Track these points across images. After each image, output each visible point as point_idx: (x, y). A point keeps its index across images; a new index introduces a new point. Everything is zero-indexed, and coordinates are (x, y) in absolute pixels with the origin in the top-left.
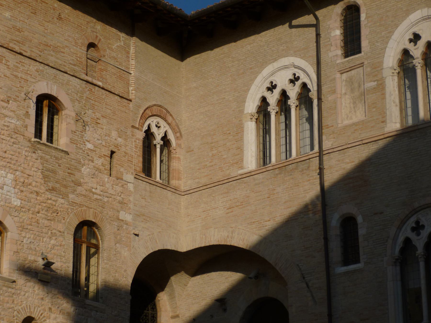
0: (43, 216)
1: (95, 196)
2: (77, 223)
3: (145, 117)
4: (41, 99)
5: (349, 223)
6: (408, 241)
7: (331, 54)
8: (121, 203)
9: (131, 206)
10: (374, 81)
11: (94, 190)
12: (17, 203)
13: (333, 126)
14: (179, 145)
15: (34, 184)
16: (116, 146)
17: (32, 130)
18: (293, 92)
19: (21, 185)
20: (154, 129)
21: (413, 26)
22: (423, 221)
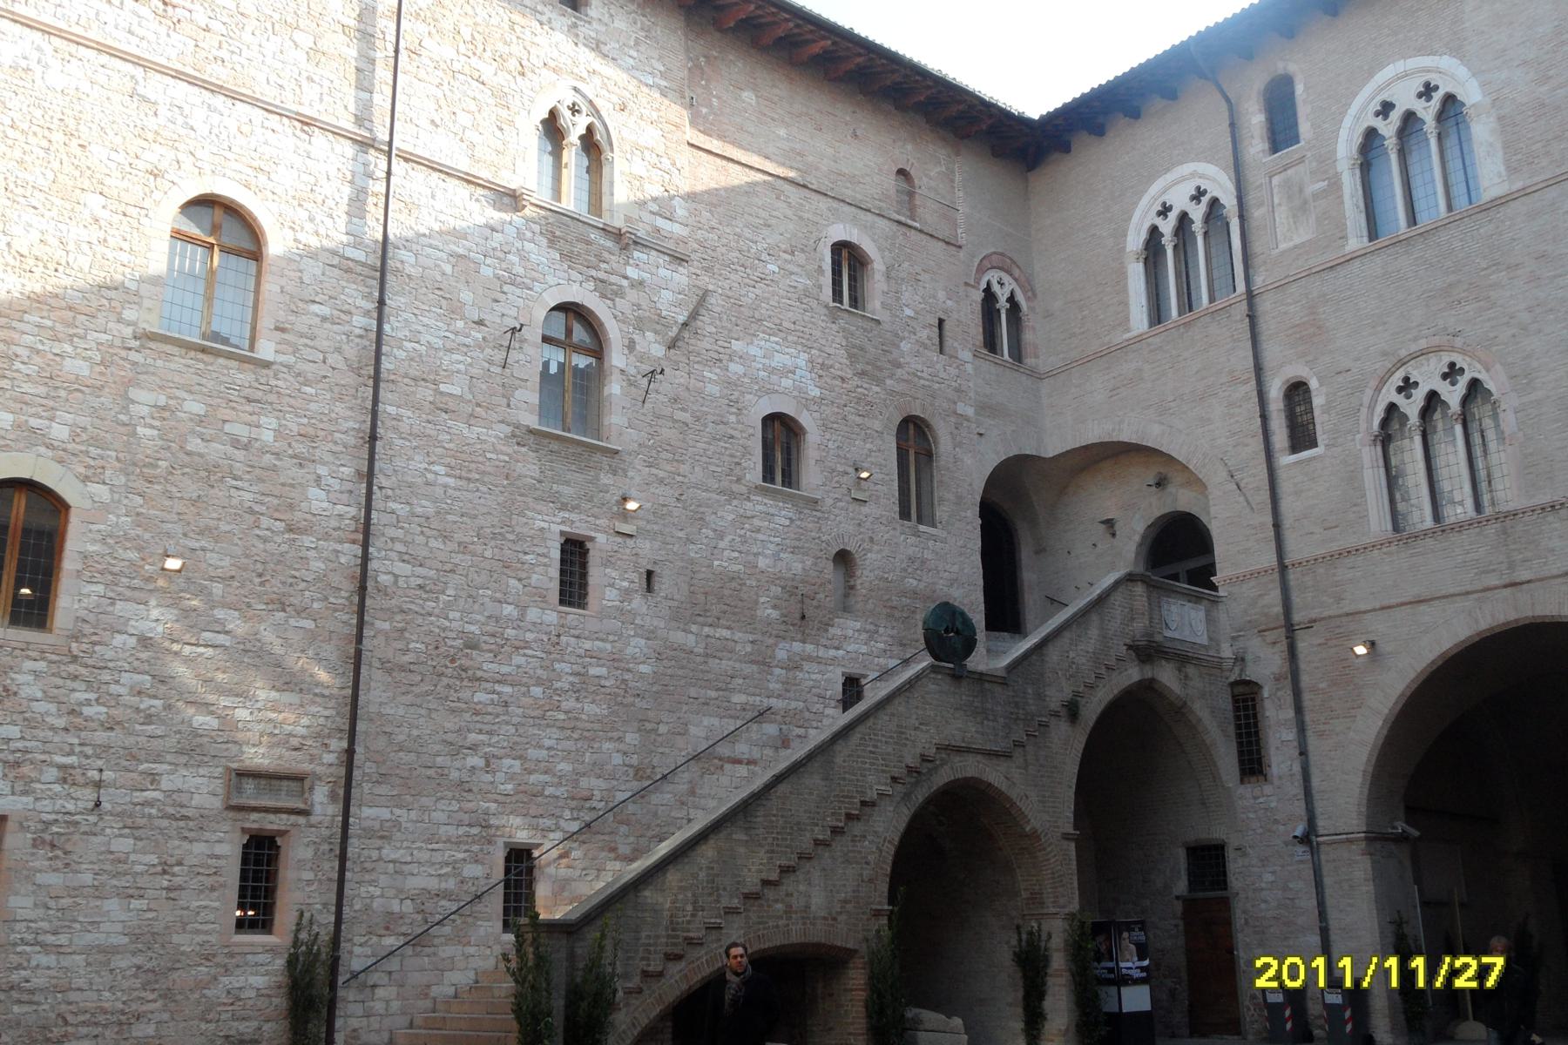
3: (981, 270)
4: (840, 248)
5: (1297, 391)
6: (1392, 408)
8: (958, 390)
9: (972, 394)
12: (816, 392)
14: (1031, 309)
16: (945, 311)
17: (828, 291)
18: (1197, 213)
19: (821, 368)
20: (996, 288)
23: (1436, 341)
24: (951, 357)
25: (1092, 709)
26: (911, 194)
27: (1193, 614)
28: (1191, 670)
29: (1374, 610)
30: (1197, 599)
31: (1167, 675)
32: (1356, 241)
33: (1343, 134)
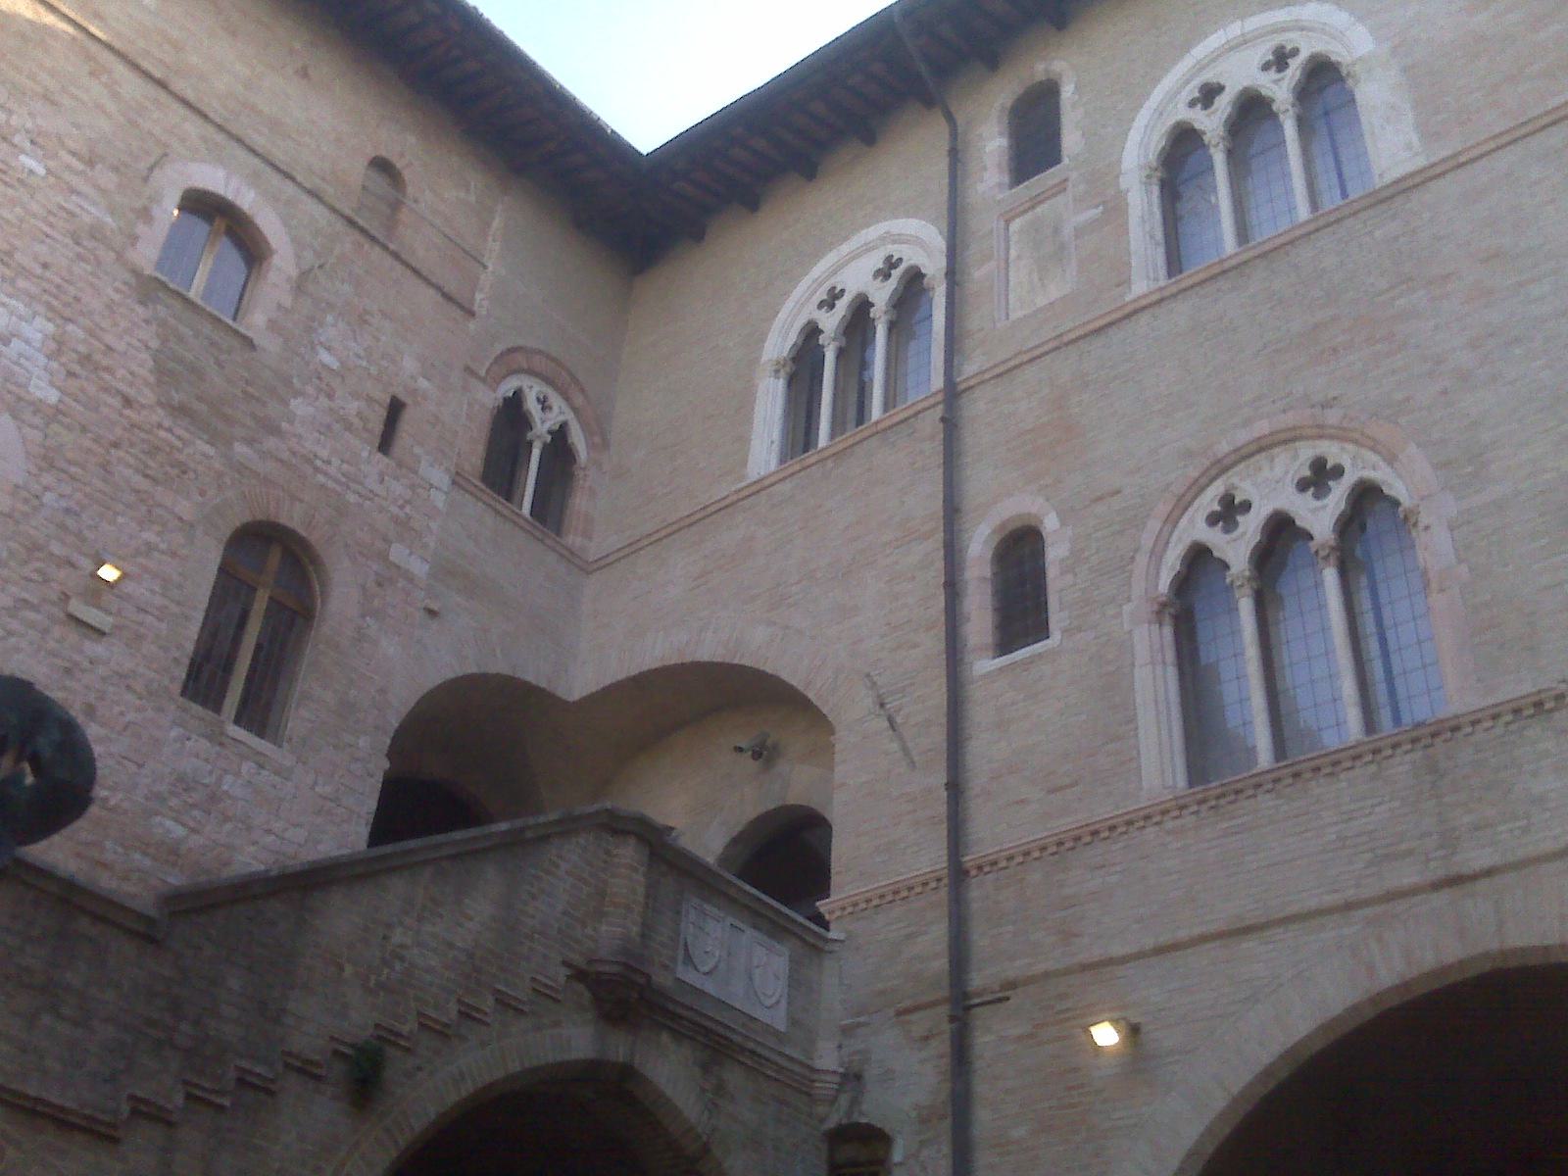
0: (132, 461)
1: (321, 478)
2: (247, 518)
7: (981, 188)
10: (1097, 206)
11: (318, 463)
13: (982, 329)
15: (121, 373)
16: (414, 392)
20: (532, 405)
21: (1202, 68)
22: (1245, 490)
23: (1289, 419)
24: (400, 465)
25: (430, 1091)
26: (396, 206)
27: (760, 954)
28: (734, 1077)
29: (1140, 955)
30: (777, 929)
31: (669, 1071)
32: (1145, 272)
33: (1134, 136)
